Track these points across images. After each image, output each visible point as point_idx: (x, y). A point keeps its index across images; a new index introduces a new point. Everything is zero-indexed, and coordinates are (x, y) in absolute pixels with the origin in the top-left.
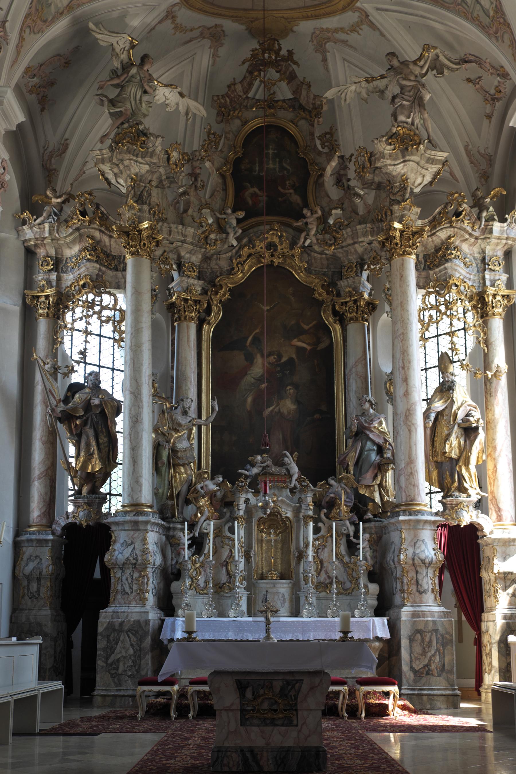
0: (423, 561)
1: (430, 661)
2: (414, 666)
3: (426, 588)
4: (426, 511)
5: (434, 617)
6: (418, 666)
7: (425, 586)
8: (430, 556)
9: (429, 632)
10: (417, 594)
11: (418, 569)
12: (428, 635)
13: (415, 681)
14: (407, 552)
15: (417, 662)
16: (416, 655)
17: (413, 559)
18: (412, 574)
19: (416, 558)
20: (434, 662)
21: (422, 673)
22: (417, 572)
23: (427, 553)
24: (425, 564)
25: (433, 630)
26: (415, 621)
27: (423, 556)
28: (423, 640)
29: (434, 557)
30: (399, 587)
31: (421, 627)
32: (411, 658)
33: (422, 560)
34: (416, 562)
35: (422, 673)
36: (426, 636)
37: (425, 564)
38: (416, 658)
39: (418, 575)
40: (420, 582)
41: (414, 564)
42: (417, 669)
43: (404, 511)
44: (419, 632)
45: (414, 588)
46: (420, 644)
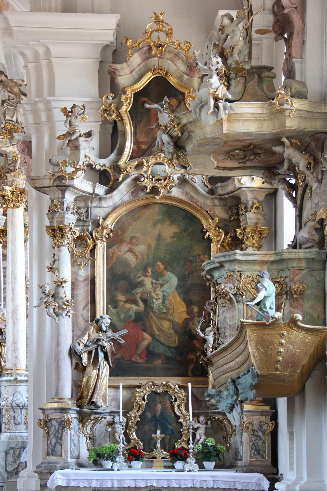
0: (18, 405)
1: (18, 466)
2: (8, 469)
3: (20, 421)
4: (22, 374)
5: (23, 439)
6: (10, 469)
7: (20, 420)
8: (24, 402)
9: (18, 449)
10: (14, 425)
11: (15, 410)
12: (18, 450)
13: (8, 478)
14: (8, 400)
15: (10, 467)
16: (9, 463)
17: (12, 404)
18: (11, 413)
19: (13, 403)
20: (21, 466)
21: (13, 473)
22: (14, 412)
23: (21, 400)
24: (19, 407)
25: (21, 447)
26: (10, 442)
27: (18, 402)
28: (14, 453)
29: (26, 403)
30: (4, 421)
31: (13, 445)
32: (6, 464)
33: (17, 405)
34: (13, 405)
35: (13, 473)
36: (16, 451)
37: (19, 407)
38: (9, 464)
39: (15, 413)
40: (16, 418)
41: (12, 407)
42: (9, 470)
43: (8, 374)
44: (12, 448)
45: (12, 421)
46: (13, 456)
